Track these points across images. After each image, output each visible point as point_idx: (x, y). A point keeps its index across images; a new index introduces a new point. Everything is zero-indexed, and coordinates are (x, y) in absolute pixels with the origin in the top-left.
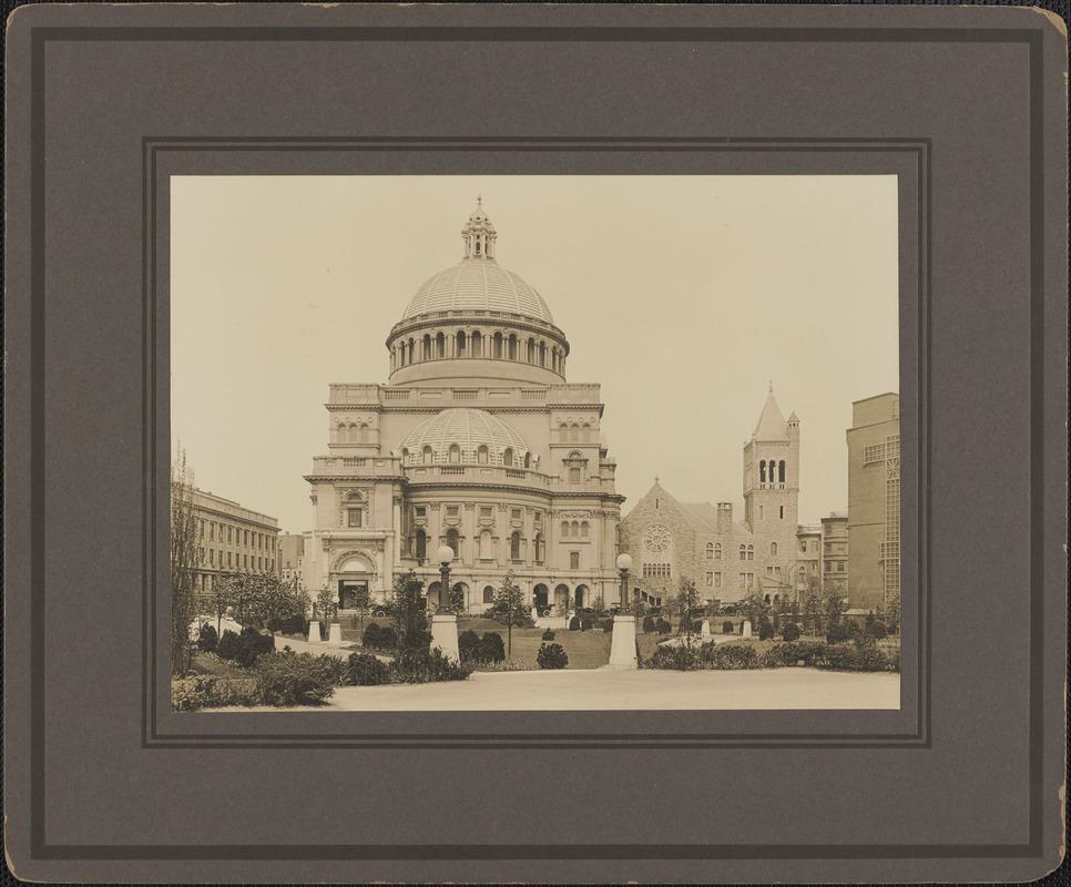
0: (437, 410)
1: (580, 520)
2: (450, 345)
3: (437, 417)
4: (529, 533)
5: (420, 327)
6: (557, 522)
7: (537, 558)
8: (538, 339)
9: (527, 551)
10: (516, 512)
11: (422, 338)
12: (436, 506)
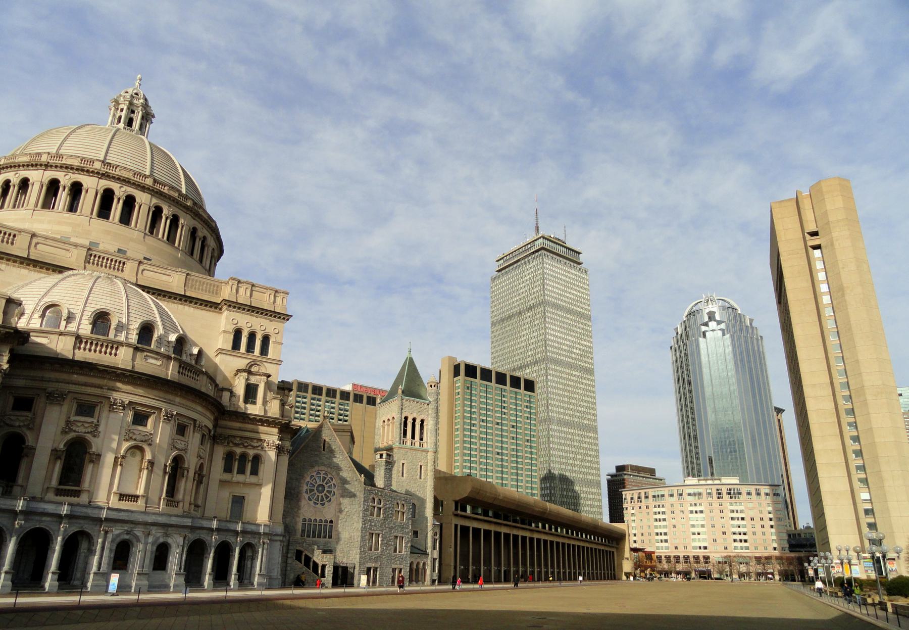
0: (59, 269)
1: (251, 452)
2: (88, 201)
3: (60, 276)
4: (191, 462)
5: (47, 166)
6: (220, 452)
7: (195, 499)
8: (202, 232)
9: (185, 487)
10: (181, 430)
11: (46, 181)
12: (56, 398)
